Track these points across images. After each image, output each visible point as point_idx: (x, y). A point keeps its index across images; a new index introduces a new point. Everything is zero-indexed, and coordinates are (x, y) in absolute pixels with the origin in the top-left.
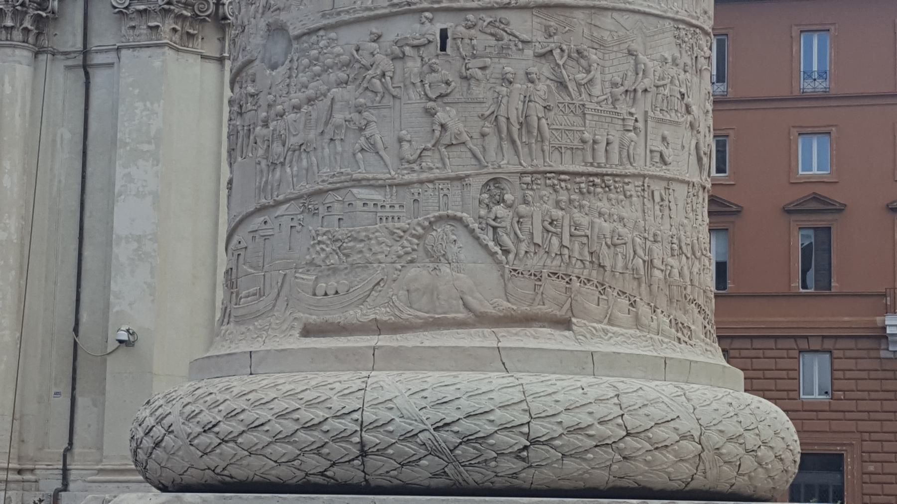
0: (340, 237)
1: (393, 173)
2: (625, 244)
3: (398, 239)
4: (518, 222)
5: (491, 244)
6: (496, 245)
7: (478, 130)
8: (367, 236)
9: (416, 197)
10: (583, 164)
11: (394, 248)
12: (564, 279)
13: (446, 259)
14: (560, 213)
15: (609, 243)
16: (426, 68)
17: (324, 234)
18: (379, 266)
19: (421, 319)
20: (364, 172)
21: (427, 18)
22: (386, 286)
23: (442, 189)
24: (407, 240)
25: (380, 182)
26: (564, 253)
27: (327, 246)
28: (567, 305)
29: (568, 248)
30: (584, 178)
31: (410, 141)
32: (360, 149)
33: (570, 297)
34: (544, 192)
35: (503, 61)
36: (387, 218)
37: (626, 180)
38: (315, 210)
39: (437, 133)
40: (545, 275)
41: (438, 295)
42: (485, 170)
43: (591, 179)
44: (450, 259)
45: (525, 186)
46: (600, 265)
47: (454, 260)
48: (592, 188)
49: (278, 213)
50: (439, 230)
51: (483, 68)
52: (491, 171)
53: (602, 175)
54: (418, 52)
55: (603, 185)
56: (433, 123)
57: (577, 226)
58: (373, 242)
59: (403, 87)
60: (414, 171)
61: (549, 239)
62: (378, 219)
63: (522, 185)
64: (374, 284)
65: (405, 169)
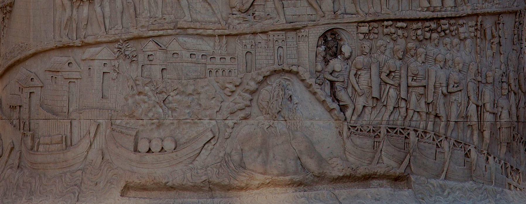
2: (461, 90)
3: (230, 94)
4: (355, 75)
5: (329, 100)
6: (334, 101)
8: (195, 90)
10: (420, 9)
12: (403, 134)
14: (398, 63)
15: (445, 91)
22: (218, 144)
24: (239, 95)
25: (210, 32)
26: (402, 106)
28: (407, 160)
29: (406, 101)
30: (420, 24)
33: (409, 152)
34: (380, 42)
37: (461, 22)
40: (383, 131)
43: (427, 24)
45: (362, 36)
46: (437, 116)
48: (428, 35)
53: (438, 19)
55: (439, 30)
57: (415, 77)
61: (386, 92)
62: (208, 71)
64: (205, 143)
65: (238, 18)
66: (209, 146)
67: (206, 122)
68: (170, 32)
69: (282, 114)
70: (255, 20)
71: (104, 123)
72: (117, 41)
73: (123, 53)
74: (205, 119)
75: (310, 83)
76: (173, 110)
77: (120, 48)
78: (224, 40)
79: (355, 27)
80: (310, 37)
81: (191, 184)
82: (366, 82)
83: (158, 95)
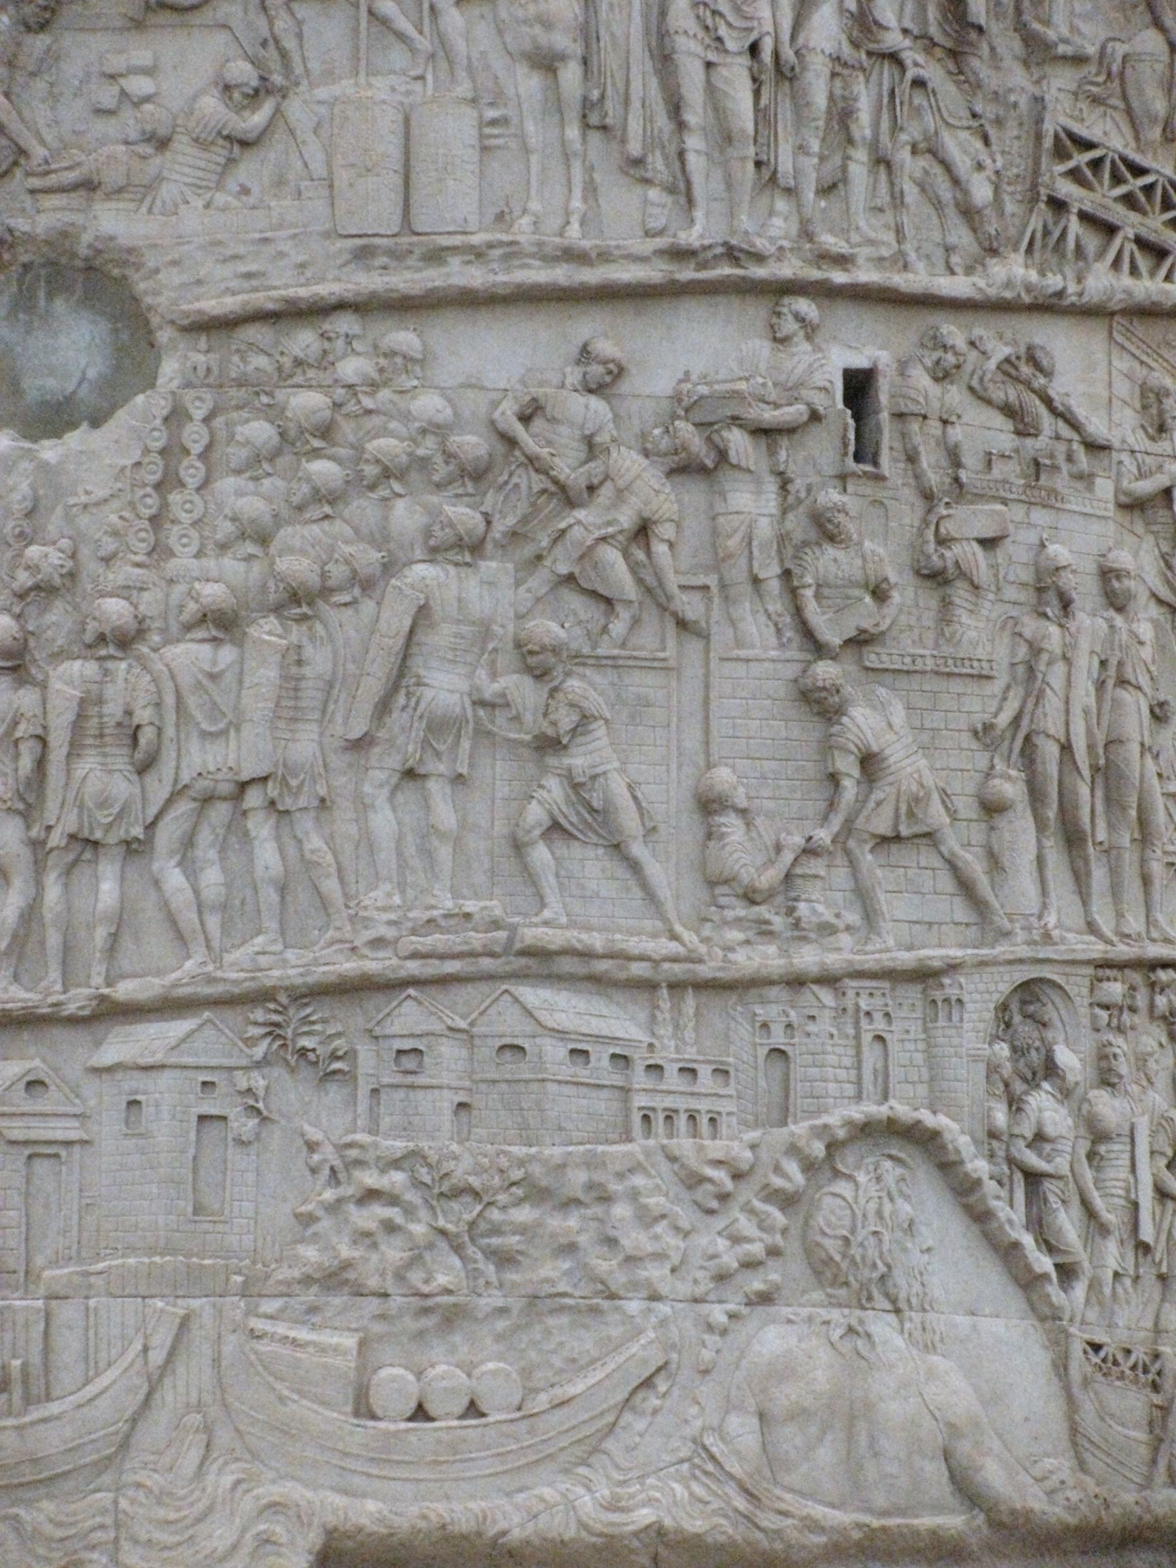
0: (475, 1182)
1: (688, 936)
3: (714, 1204)
7: (971, 788)
8: (590, 1186)
9: (778, 1038)
11: (702, 1241)
13: (887, 1295)
16: (797, 525)
17: (396, 1164)
18: (649, 1310)
19: (822, 1530)
20: (564, 920)
21: (800, 318)
22: (676, 1392)
23: (868, 1014)
25: (638, 969)
27: (409, 1211)
31: (743, 812)
32: (547, 823)
35: (1040, 516)
36: (668, 1118)
38: (334, 1057)
39: (850, 788)
41: (872, 1440)
42: (1002, 950)
44: (902, 1295)
45: (1104, 1015)
47: (914, 1301)
49: (110, 1053)
50: (862, 1178)
51: (988, 543)
52: (1024, 951)
54: (772, 452)
56: (827, 747)
58: (621, 1210)
59: (715, 590)
60: (771, 933)
62: (637, 1118)
63: (1097, 1010)
66: (644, 1400)
67: (634, 1306)
68: (486, 963)
69: (890, 1284)
70: (796, 933)
71: (208, 1310)
72: (263, 996)
73: (289, 1043)
74: (630, 1295)
75: (975, 1176)
76: (505, 1259)
77: (277, 1025)
78: (690, 1002)
79: (1087, 982)
80: (969, 1006)
81: (594, 1539)
82: (1122, 1184)
83: (443, 1201)
